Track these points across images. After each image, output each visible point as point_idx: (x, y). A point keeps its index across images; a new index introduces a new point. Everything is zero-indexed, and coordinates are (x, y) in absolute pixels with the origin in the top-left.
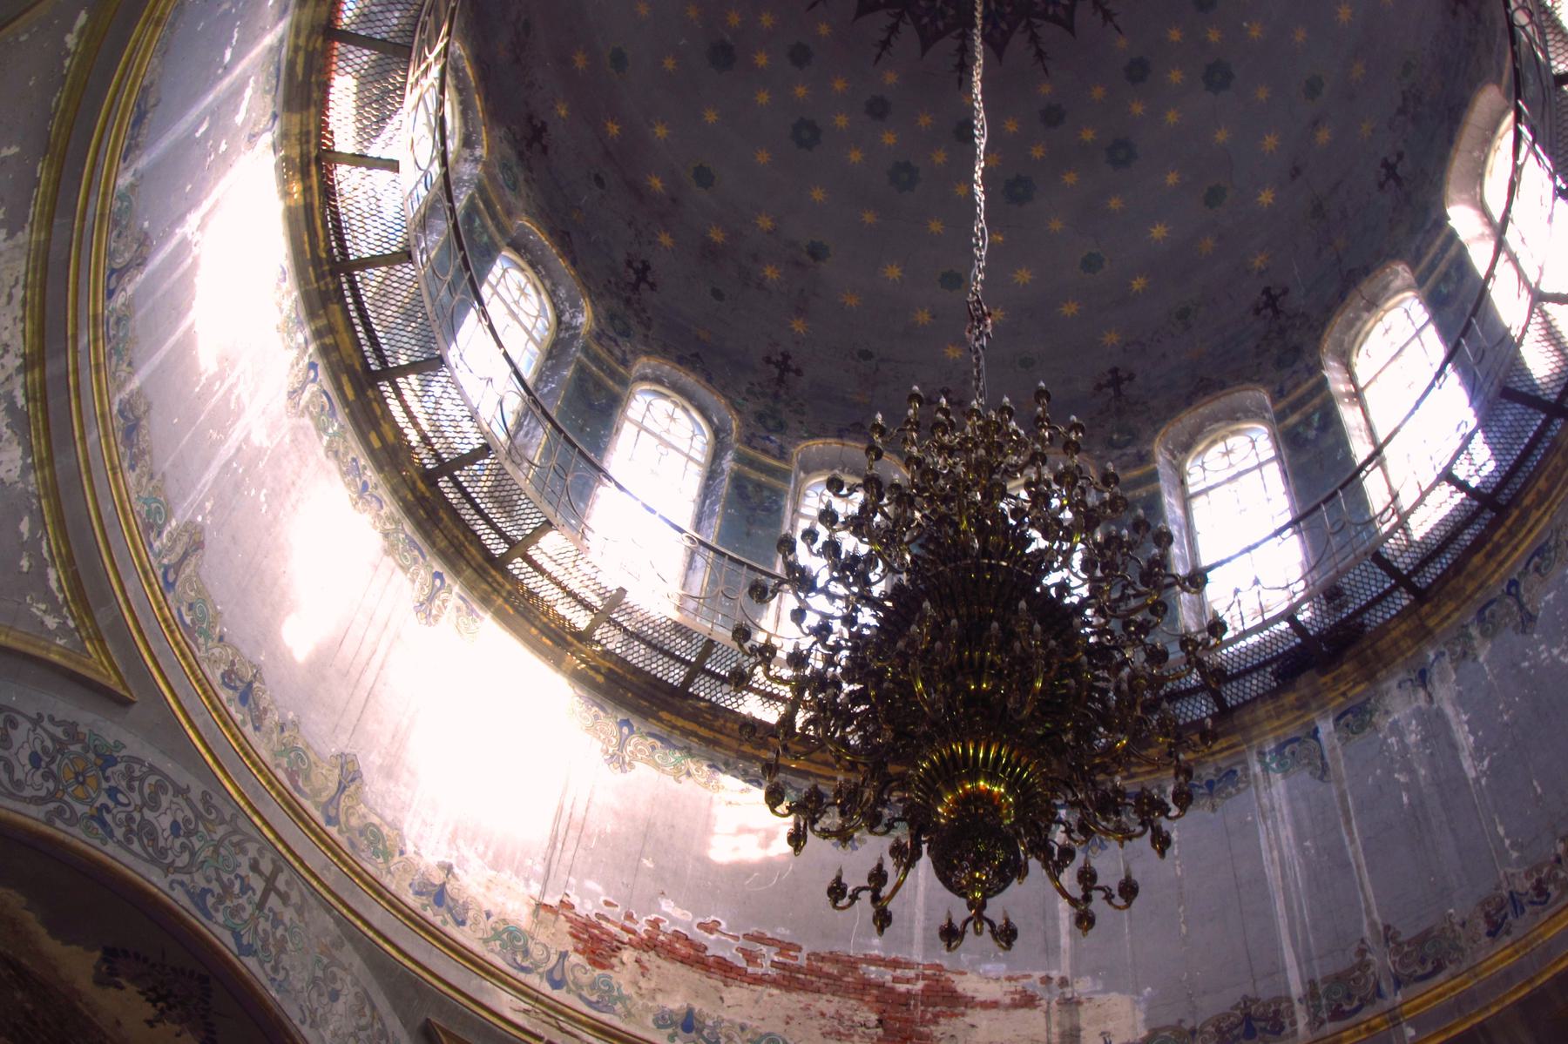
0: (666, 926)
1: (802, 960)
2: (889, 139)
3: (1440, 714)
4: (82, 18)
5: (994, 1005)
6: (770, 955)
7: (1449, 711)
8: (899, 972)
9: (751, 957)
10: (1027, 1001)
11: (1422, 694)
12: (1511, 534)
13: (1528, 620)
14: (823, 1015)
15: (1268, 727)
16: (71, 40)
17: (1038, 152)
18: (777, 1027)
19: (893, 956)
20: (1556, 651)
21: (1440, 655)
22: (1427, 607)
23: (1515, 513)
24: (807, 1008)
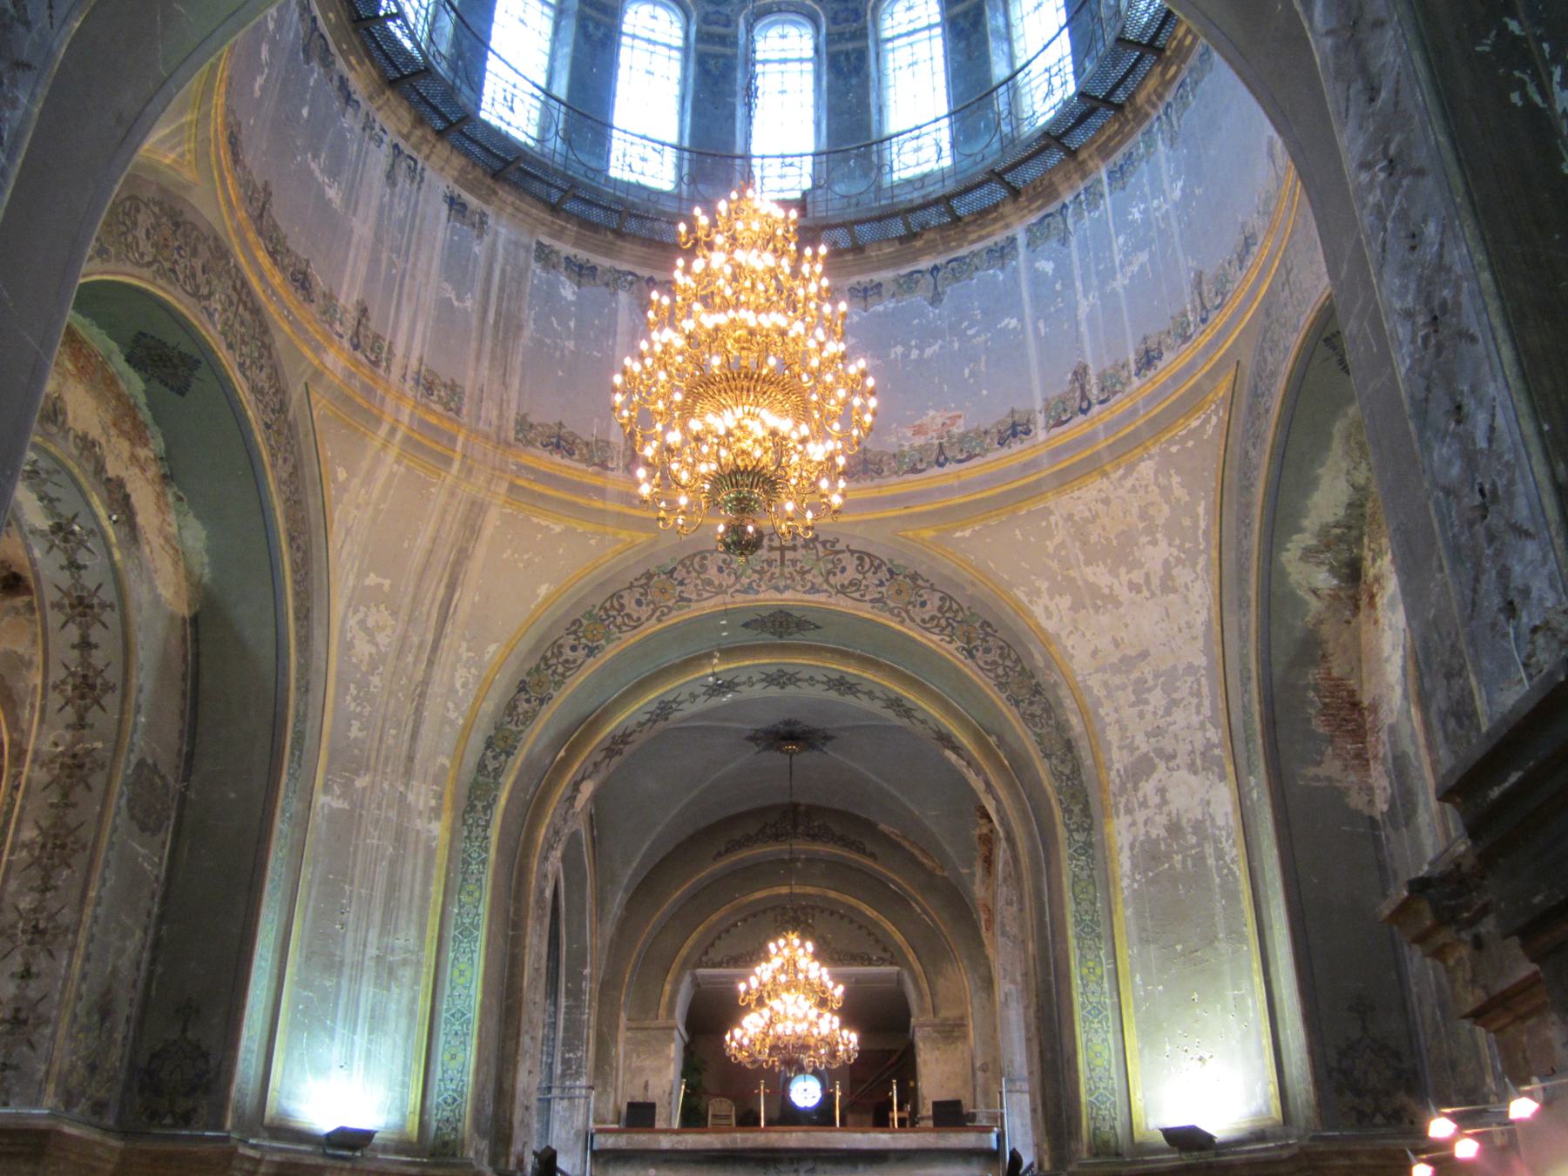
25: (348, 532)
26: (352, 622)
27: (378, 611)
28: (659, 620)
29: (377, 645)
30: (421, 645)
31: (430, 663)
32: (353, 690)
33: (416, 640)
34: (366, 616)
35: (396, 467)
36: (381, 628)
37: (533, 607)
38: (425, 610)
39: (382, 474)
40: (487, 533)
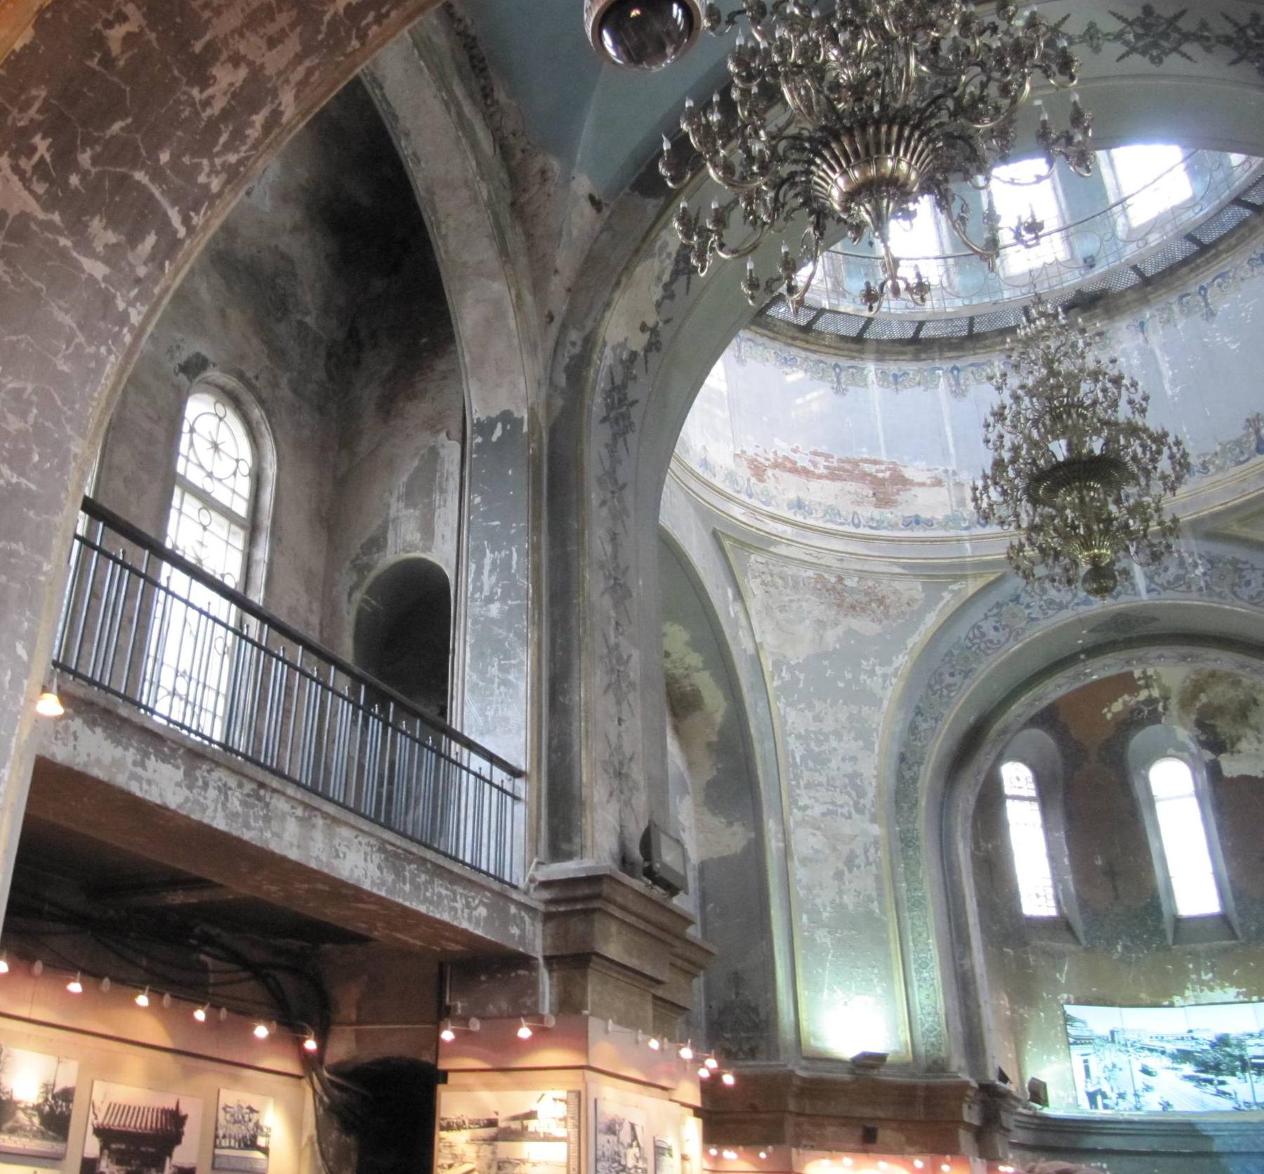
0: (780, 454)
1: (835, 464)
3: (1152, 352)
5: (923, 484)
6: (822, 462)
7: (1158, 352)
9: (815, 464)
10: (938, 483)
11: (1141, 336)
12: (1208, 262)
13: (1211, 314)
18: (831, 501)
19: (873, 457)
20: (1226, 340)
21: (1152, 316)
23: (1213, 251)
24: (842, 490)
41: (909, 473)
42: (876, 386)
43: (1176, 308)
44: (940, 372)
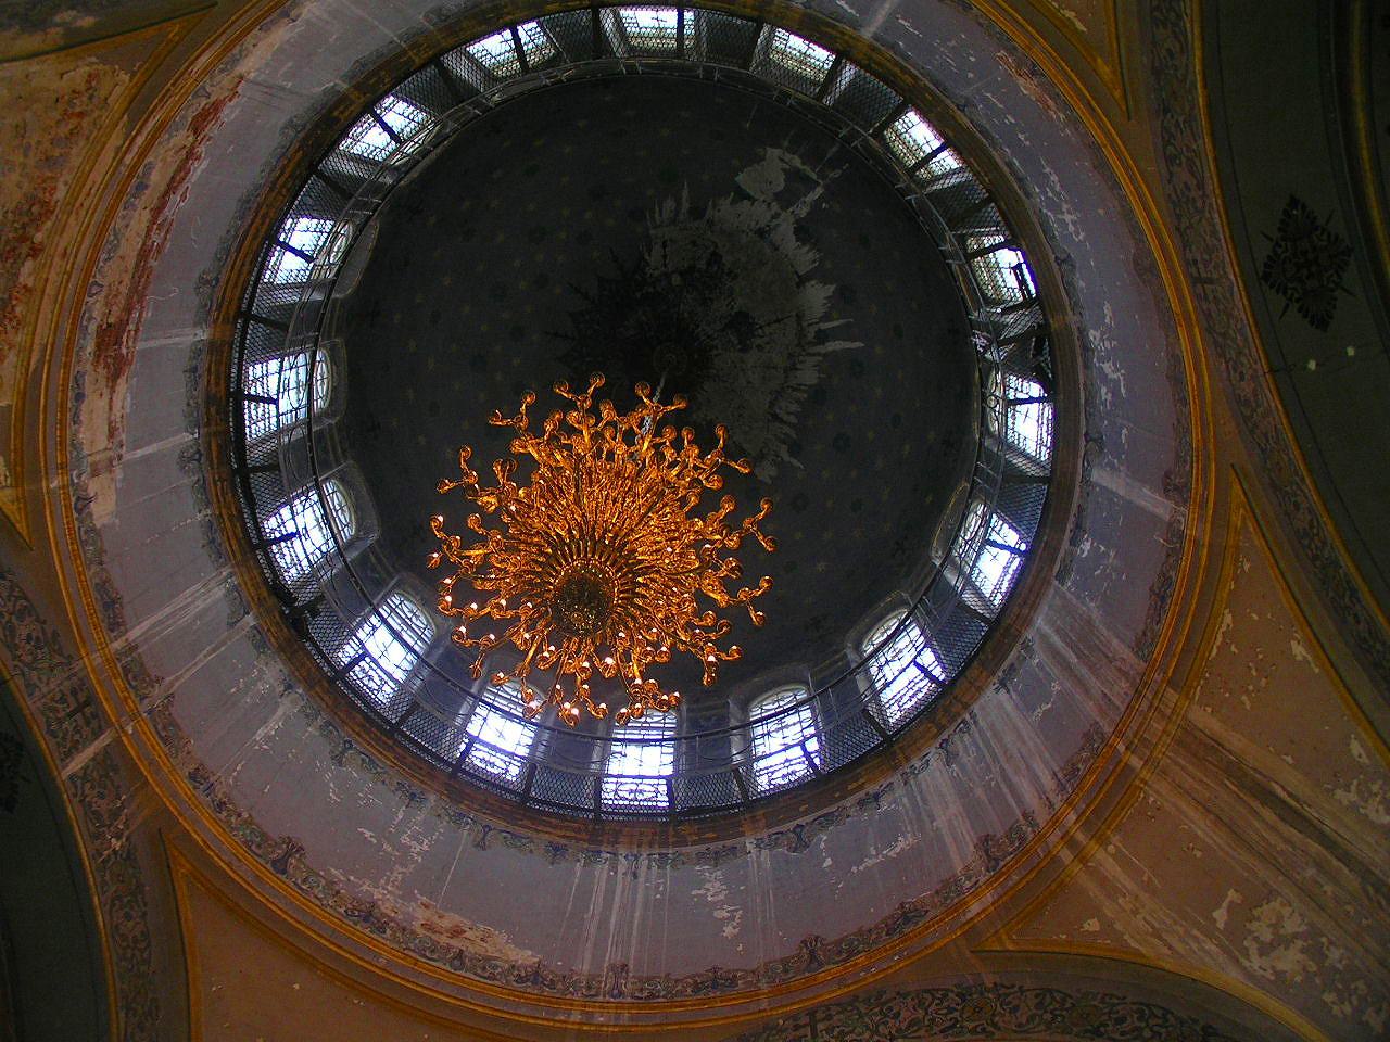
2: (523, 285)
4: (1080, 26)
7: (280, 712)
8: (133, 333)
10: (111, 434)
14: (120, 283)
15: (246, 578)
16: (1070, 14)
17: (499, 377)
22: (326, 685)
23: (390, 743)
25: (1157, 934)
26: (1255, 963)
27: (1258, 919)
28: (1303, 479)
29: (1296, 936)
30: (1319, 865)
31: (1345, 858)
32: (1329, 997)
33: (1311, 872)
34: (1256, 939)
35: (1111, 848)
36: (1275, 927)
37: (1317, 670)
38: (1281, 846)
39: (1112, 868)
40: (1215, 726)
41: (122, 385)
42: (192, 339)
43: (320, 721)
44: (196, 436)
